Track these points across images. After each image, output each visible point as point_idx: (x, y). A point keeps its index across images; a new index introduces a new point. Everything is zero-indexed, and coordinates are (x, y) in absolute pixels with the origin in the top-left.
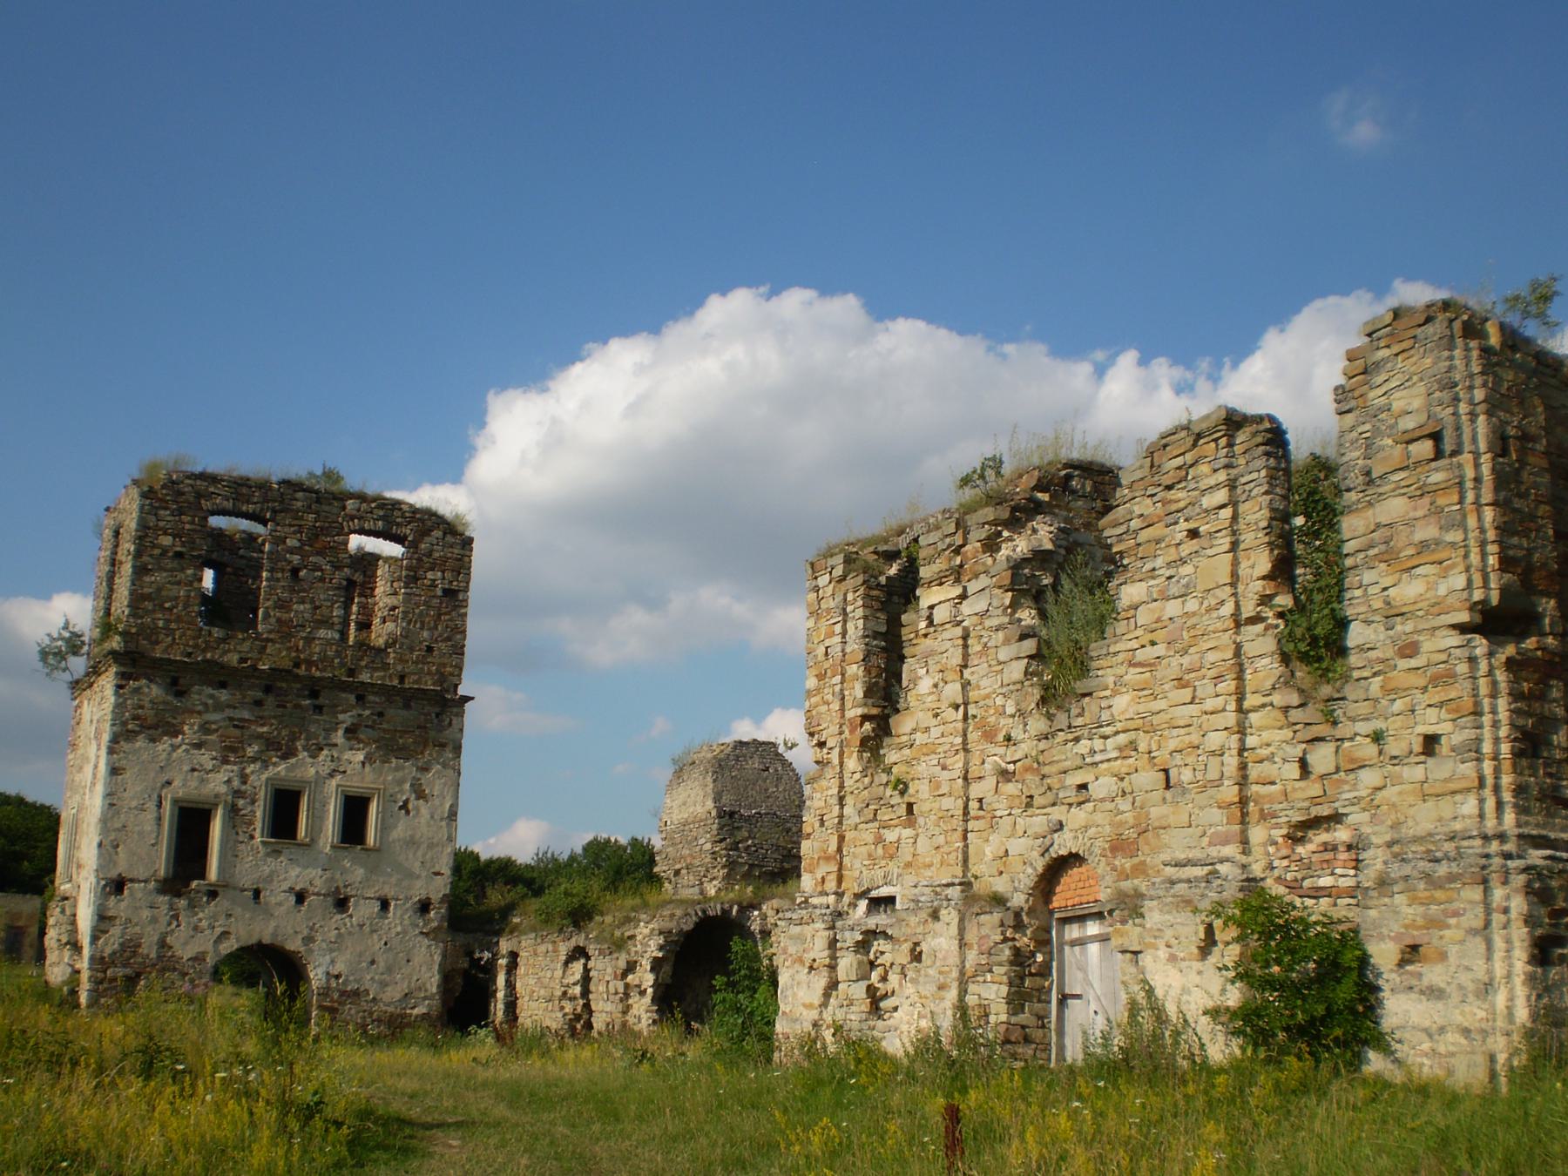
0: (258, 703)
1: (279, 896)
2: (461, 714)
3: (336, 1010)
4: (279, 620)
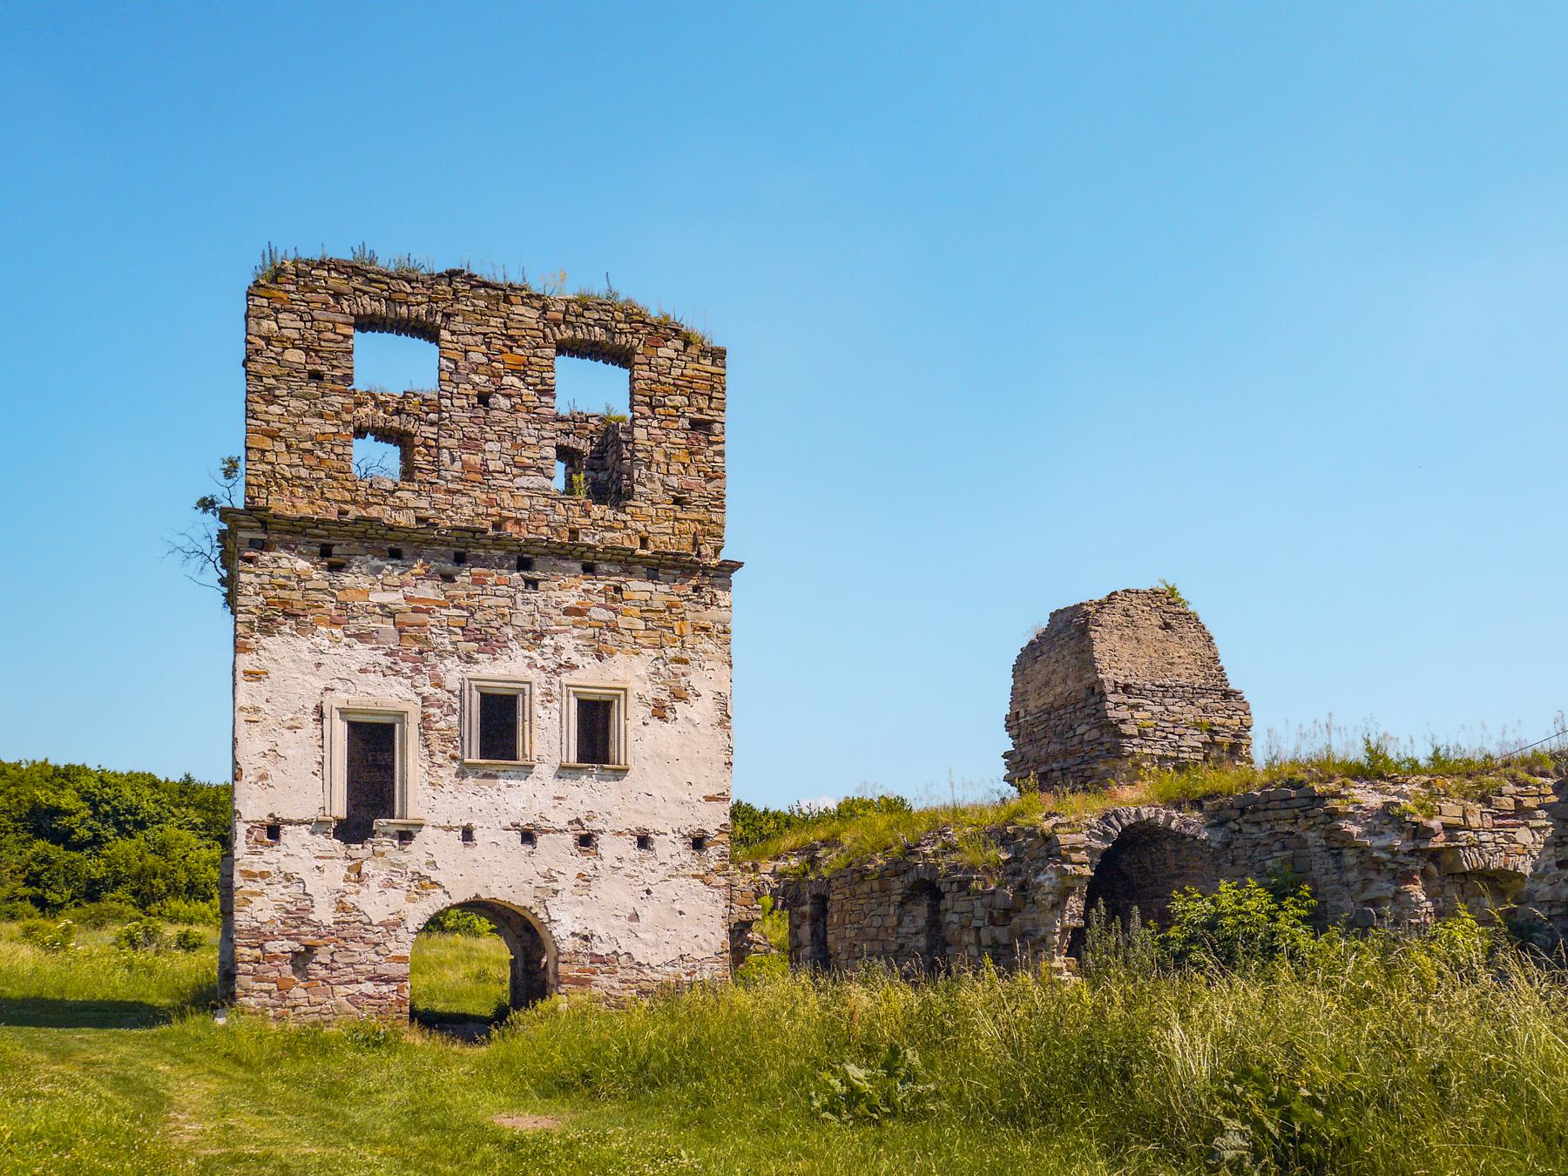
0: (448, 578)
1: (494, 838)
2: (727, 587)
3: (589, 981)
4: (464, 464)
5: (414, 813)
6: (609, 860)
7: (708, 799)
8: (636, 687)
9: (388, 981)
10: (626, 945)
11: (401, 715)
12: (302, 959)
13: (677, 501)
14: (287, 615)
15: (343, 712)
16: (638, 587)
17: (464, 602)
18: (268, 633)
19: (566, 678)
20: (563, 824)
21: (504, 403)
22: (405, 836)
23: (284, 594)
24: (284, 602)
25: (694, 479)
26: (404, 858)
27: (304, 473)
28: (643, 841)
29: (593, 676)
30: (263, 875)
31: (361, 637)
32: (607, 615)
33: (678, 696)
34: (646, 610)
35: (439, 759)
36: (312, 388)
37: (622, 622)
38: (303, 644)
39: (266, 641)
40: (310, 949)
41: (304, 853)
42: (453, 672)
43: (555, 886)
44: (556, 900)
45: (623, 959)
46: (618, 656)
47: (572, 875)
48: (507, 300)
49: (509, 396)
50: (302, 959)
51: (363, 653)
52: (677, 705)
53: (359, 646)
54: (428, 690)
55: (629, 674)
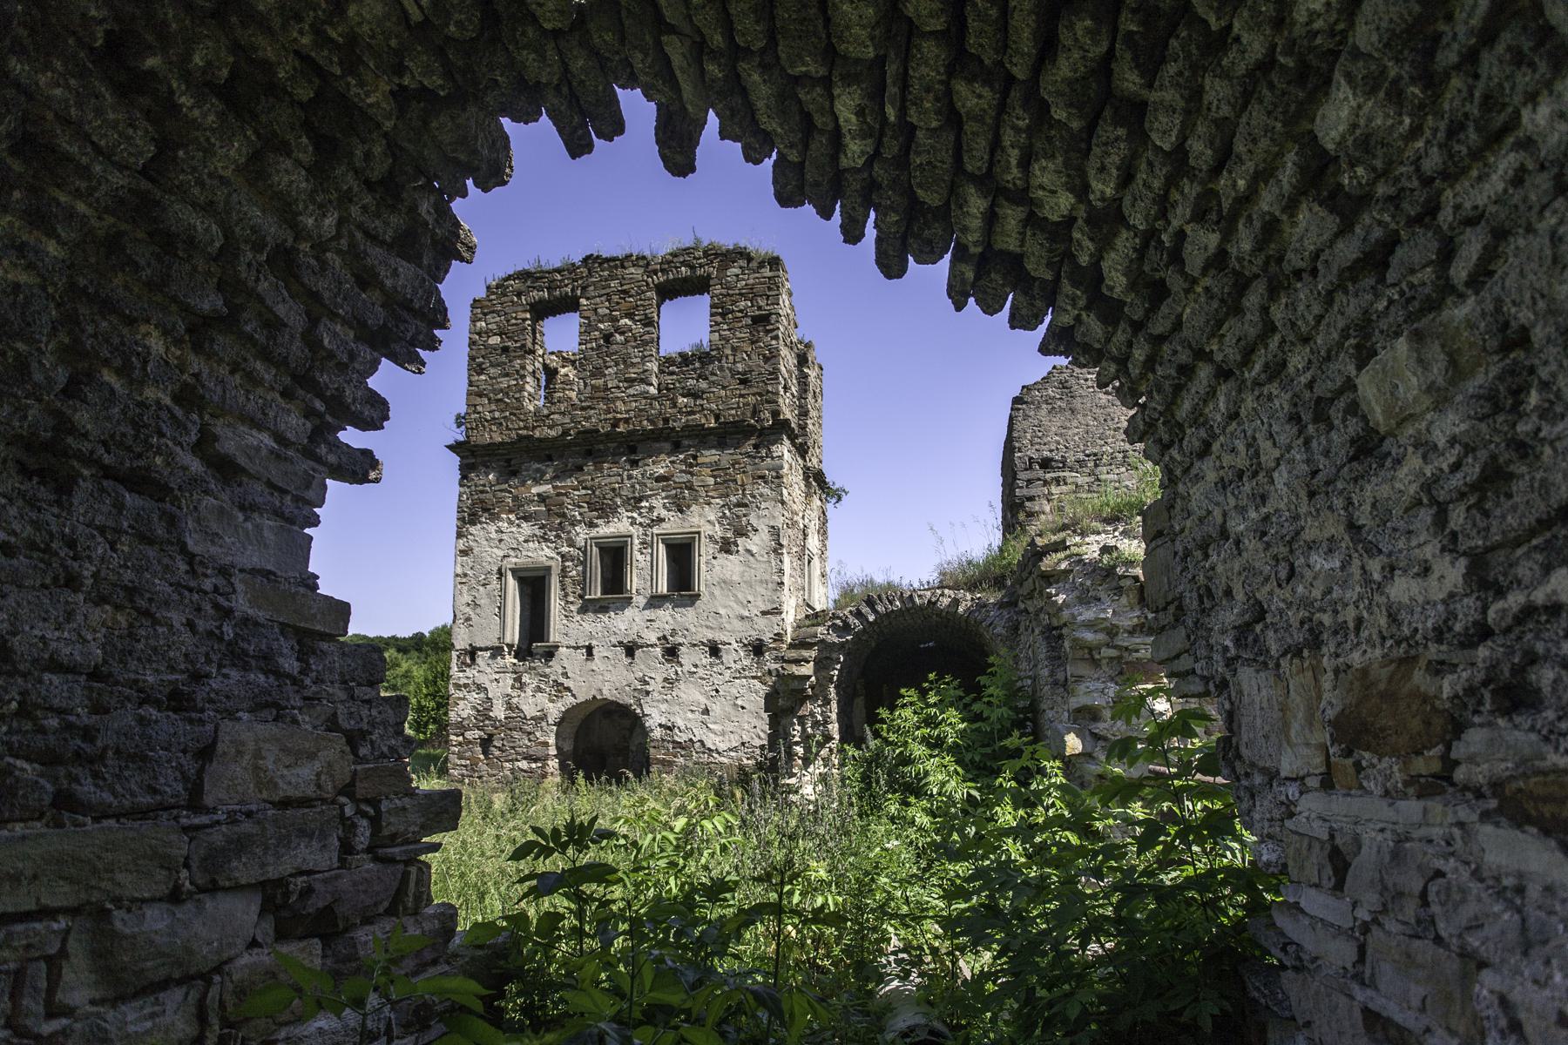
5: (554, 636)
6: (688, 667)
7: (764, 613)
8: (707, 529)
9: (535, 761)
10: (699, 733)
11: (549, 568)
12: (486, 743)
13: (744, 382)
14: (485, 510)
15: (514, 571)
16: (710, 456)
17: (589, 484)
18: (473, 523)
19: (656, 530)
20: (654, 640)
21: (618, 338)
22: (550, 654)
23: (482, 496)
24: (482, 501)
25: (757, 360)
26: (548, 670)
27: (497, 414)
28: (714, 650)
29: (674, 525)
30: (466, 686)
31: (526, 518)
32: (686, 478)
33: (741, 533)
34: (716, 468)
35: (571, 599)
36: (504, 358)
37: (696, 482)
38: (492, 528)
39: (472, 529)
40: (491, 736)
41: (489, 670)
42: (581, 534)
43: (649, 688)
44: (648, 699)
45: (697, 745)
46: (694, 508)
47: (659, 679)
48: (623, 267)
49: (622, 333)
50: (486, 743)
51: (527, 529)
52: (739, 541)
53: (524, 525)
54: (565, 549)
55: (705, 520)
